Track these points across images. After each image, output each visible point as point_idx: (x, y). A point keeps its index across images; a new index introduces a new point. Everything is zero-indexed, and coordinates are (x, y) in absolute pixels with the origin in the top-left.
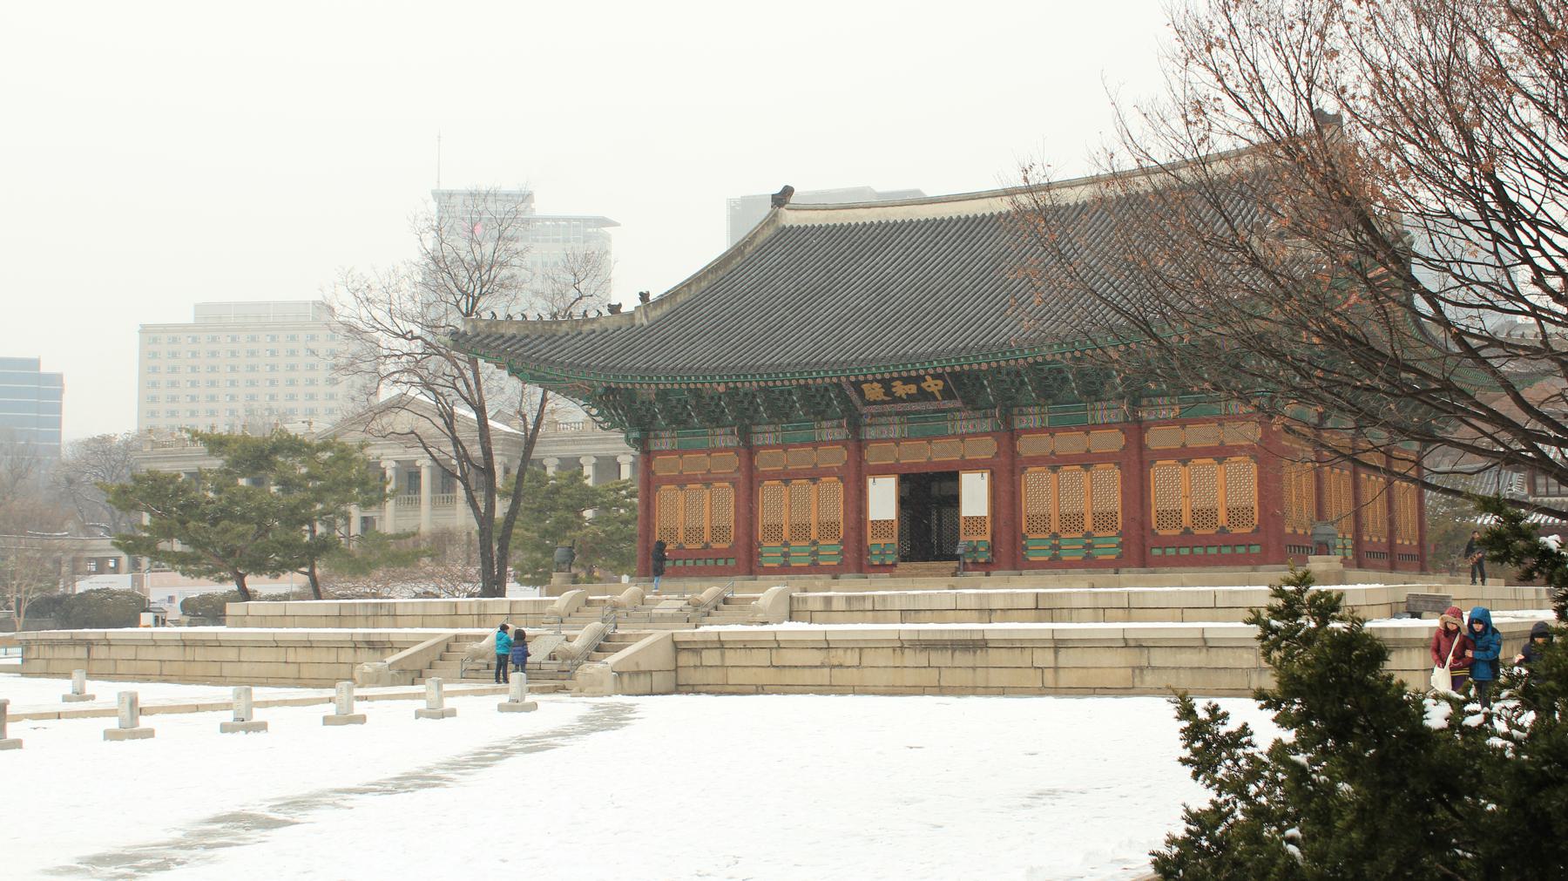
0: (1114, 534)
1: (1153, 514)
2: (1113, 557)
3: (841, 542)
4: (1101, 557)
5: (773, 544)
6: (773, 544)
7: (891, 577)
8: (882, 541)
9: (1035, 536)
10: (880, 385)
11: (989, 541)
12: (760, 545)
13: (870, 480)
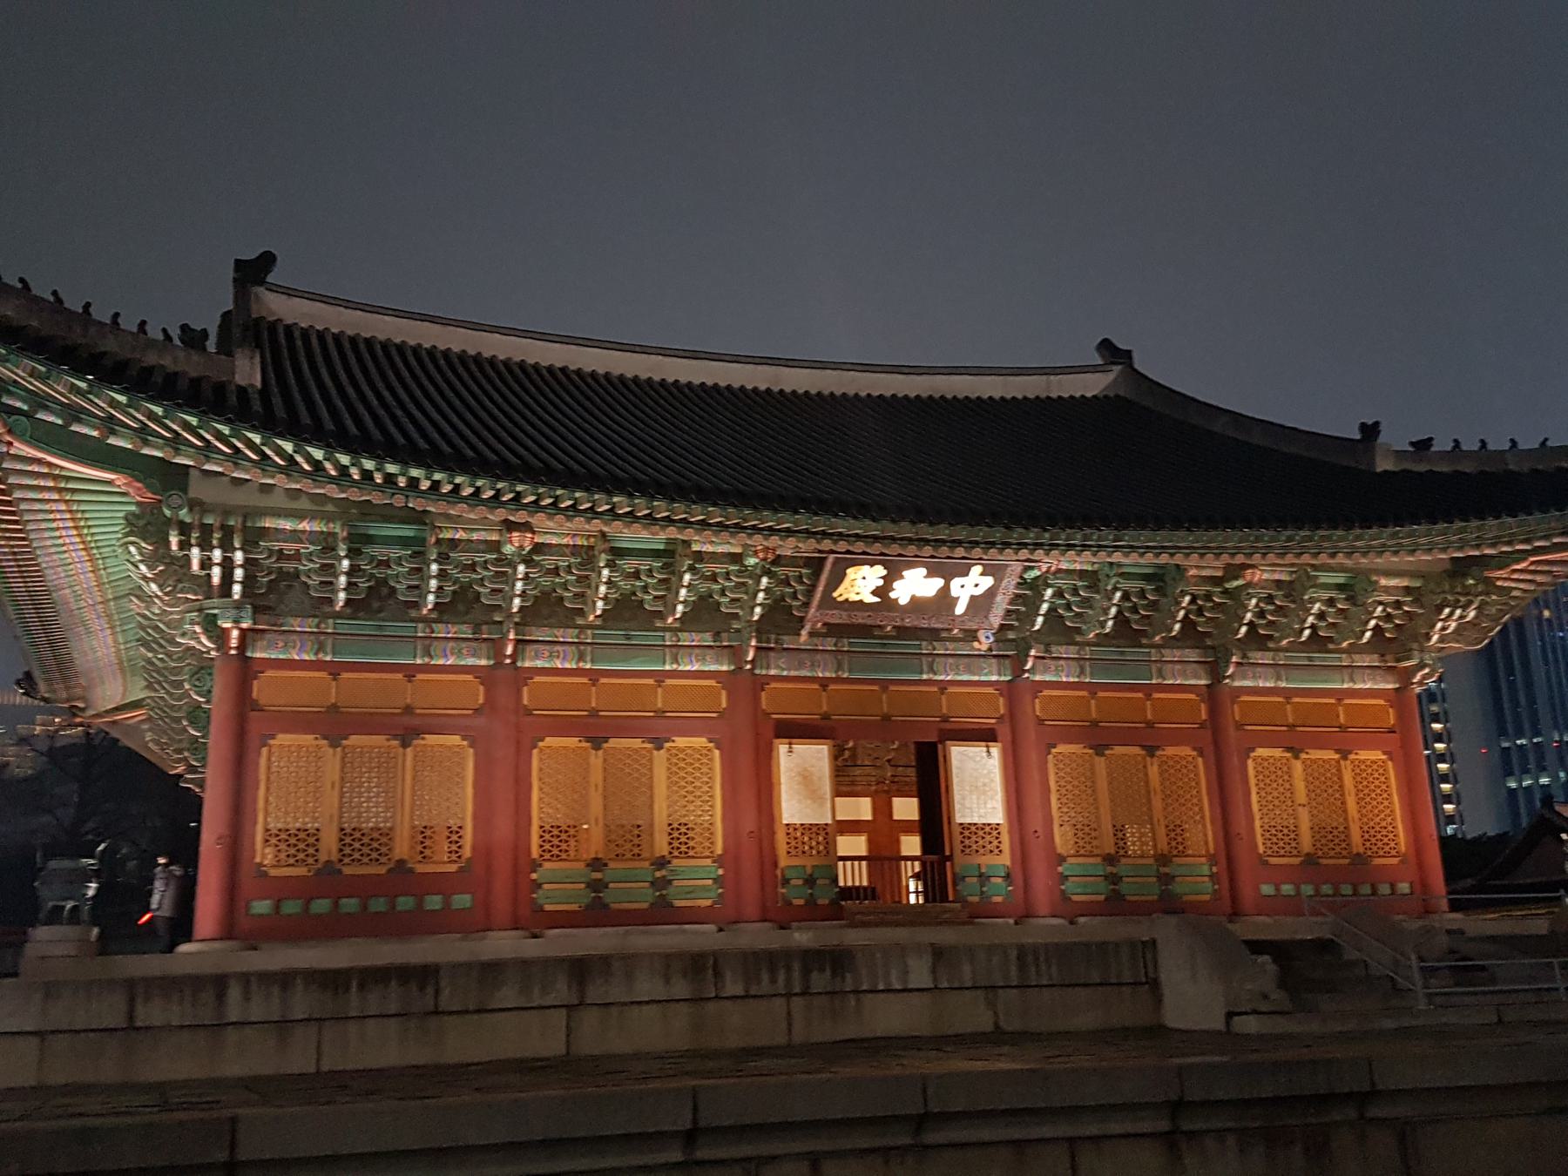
3: (719, 861)
10: (884, 572)
11: (1008, 863)
13: (782, 748)
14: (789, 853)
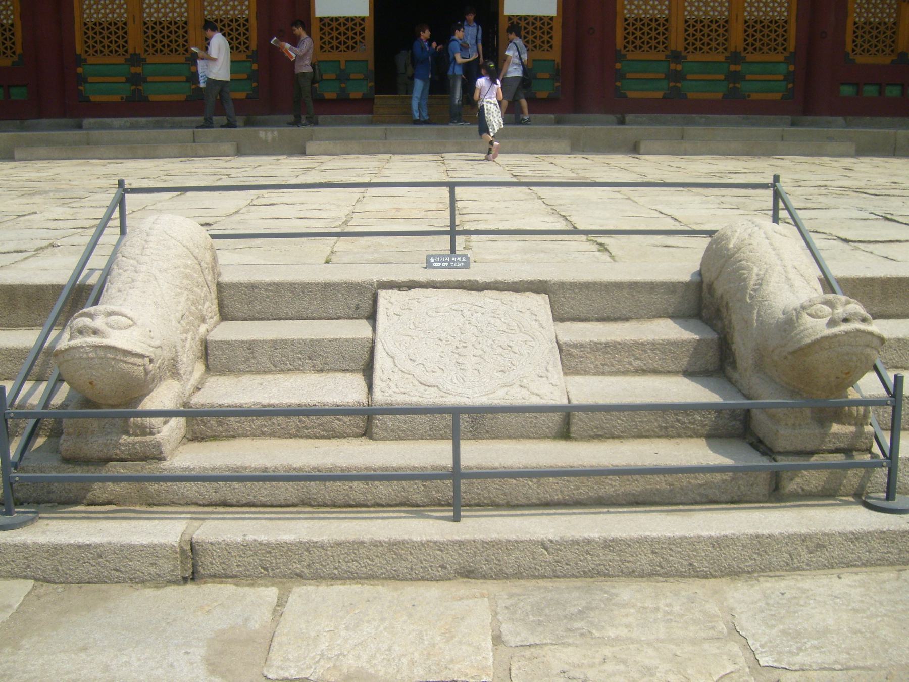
0: (781, 58)
1: (850, 28)
2: (778, 96)
4: (754, 96)
5: (107, 60)
6: (107, 60)
7: (371, 123)
8: (343, 57)
9: (637, 55)
11: (558, 60)
12: (79, 61)
14: (322, 48)
